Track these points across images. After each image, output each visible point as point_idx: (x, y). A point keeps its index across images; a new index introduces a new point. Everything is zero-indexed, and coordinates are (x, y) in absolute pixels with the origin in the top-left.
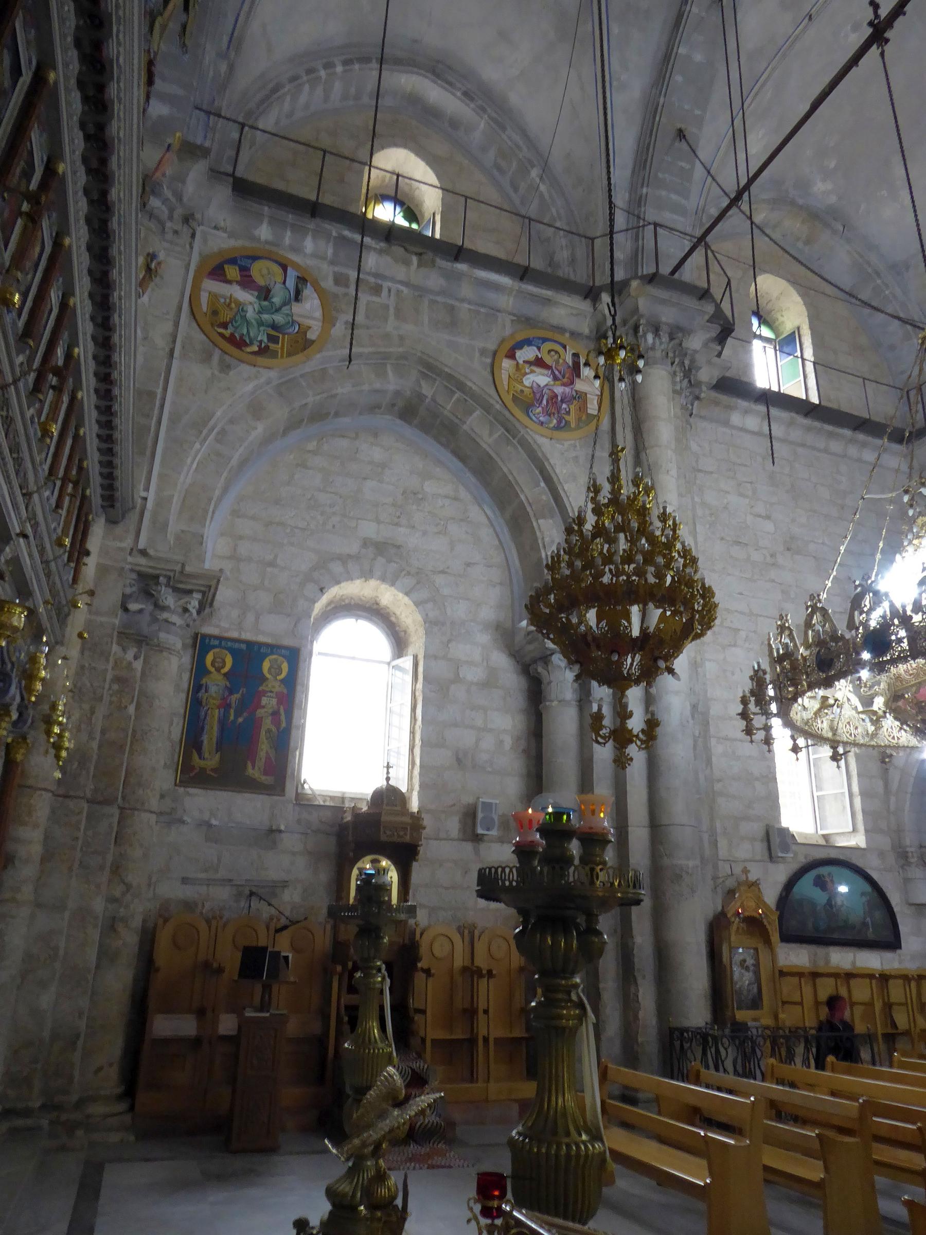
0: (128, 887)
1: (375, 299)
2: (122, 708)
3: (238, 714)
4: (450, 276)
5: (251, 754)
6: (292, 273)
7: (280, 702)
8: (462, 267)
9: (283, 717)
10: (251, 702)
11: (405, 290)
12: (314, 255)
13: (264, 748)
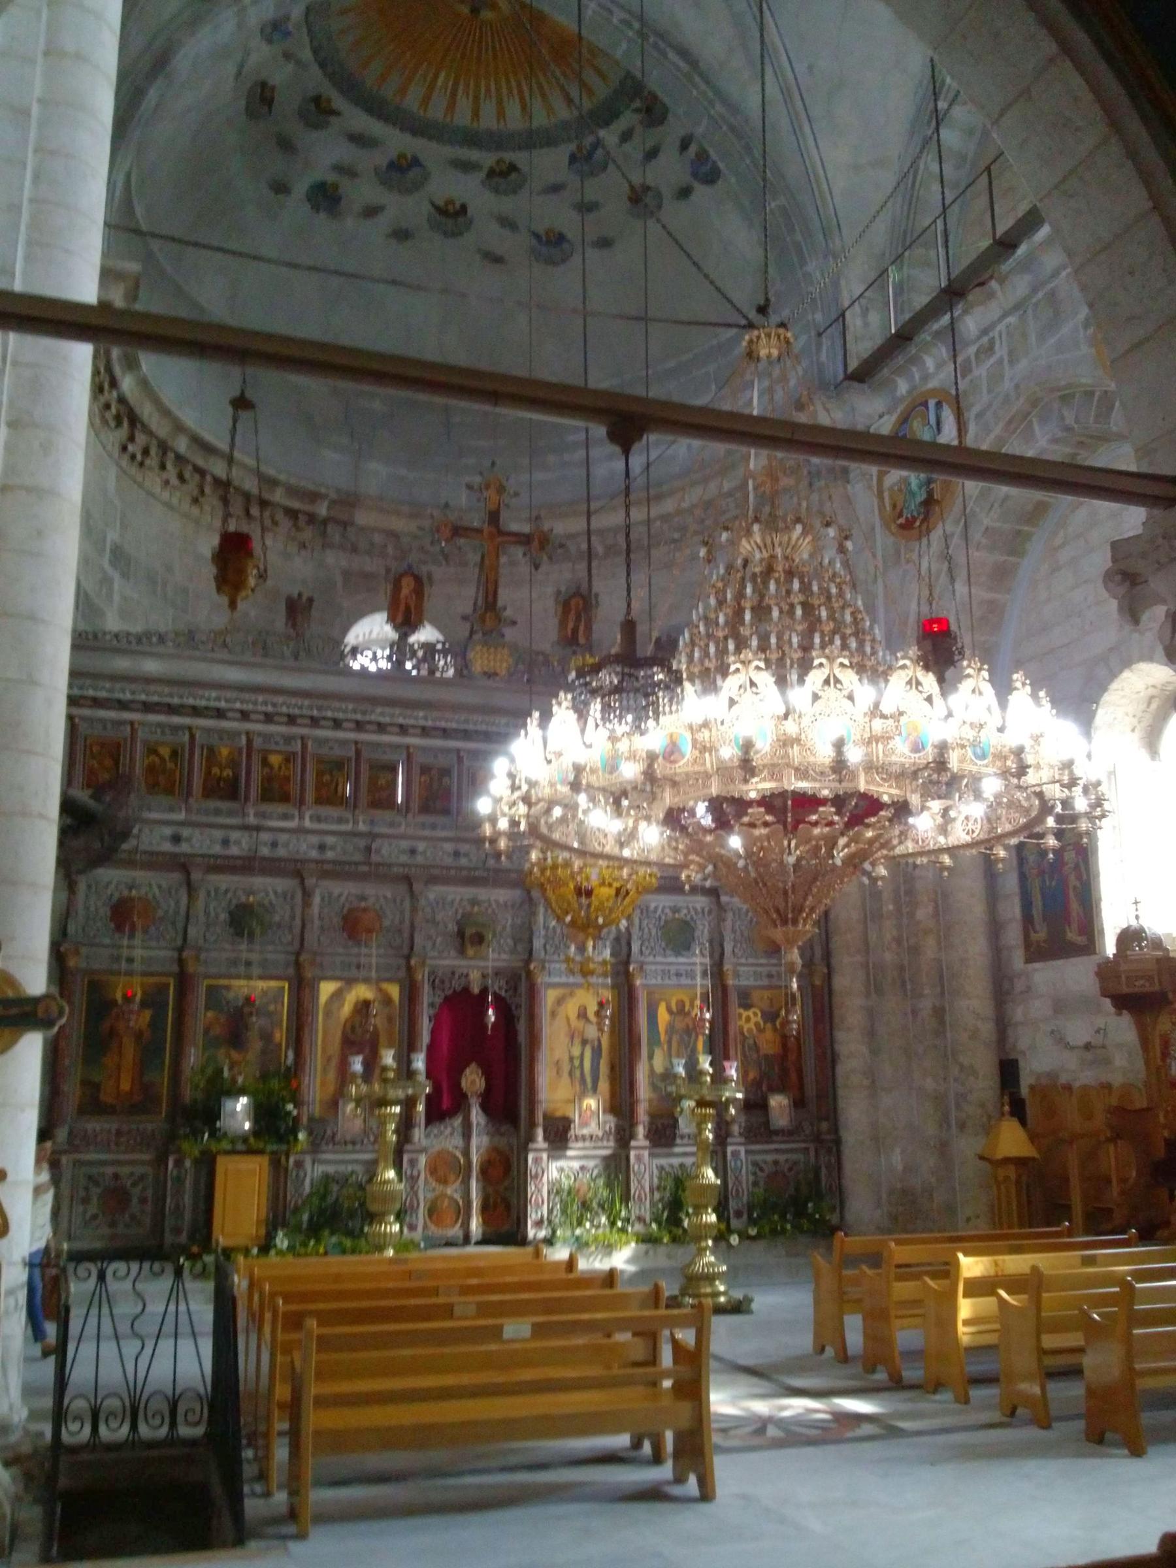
0: (962, 1066)
1: (992, 360)
2: (912, 915)
4: (1027, 265)
6: (932, 403)
8: (1022, 250)
11: (1011, 319)
12: (939, 366)
13: (1075, 906)
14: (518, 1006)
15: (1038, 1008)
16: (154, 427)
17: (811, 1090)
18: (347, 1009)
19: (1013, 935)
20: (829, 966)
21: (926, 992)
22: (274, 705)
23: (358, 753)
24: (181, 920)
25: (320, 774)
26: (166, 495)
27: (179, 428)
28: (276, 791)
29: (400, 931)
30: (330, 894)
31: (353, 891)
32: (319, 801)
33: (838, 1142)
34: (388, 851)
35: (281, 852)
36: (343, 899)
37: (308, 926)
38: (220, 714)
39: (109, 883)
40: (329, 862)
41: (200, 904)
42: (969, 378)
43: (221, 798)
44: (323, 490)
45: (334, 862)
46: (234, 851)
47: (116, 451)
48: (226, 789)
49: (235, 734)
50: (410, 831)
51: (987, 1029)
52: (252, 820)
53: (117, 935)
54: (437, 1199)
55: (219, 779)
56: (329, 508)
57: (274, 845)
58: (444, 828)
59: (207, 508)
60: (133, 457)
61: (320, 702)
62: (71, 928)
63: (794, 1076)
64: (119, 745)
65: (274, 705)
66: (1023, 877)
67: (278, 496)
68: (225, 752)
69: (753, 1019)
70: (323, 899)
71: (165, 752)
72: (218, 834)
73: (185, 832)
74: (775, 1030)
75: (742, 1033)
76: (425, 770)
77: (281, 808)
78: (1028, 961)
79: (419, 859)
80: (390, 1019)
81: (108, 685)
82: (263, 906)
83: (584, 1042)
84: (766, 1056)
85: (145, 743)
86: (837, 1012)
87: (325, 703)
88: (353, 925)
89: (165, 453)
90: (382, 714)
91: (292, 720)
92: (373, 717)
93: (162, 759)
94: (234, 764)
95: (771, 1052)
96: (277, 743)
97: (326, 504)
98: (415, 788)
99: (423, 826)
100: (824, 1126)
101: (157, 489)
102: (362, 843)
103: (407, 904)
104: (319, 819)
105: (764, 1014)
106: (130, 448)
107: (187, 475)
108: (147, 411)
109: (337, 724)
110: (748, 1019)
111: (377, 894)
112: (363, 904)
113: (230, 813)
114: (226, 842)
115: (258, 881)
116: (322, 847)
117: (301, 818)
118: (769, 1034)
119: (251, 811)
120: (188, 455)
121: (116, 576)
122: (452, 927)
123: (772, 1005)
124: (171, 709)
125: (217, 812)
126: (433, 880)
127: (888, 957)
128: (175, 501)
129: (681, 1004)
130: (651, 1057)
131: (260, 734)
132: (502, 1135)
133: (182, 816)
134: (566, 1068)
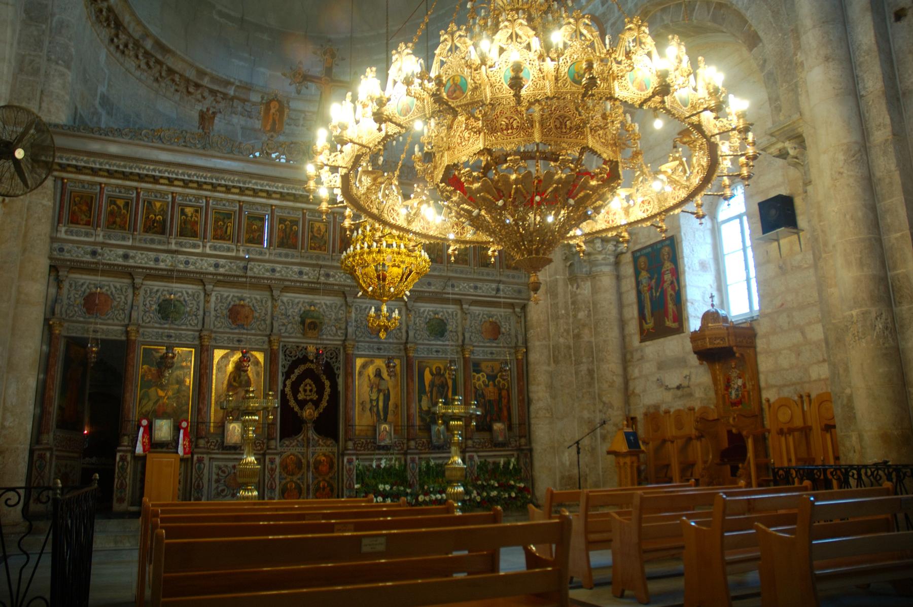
0: (604, 403)
3: (656, 291)
5: (666, 314)
7: (673, 275)
9: (676, 284)
10: (660, 282)
13: (671, 306)
14: (338, 368)
15: (649, 367)
16: (131, 30)
17: (515, 420)
18: (230, 367)
19: (633, 327)
20: (526, 348)
21: (584, 360)
22: (189, 176)
23: (241, 208)
24: (127, 307)
25: (216, 221)
26: (138, 73)
27: (147, 35)
28: (188, 230)
29: (264, 320)
30: (222, 296)
31: (236, 294)
32: (215, 238)
33: (531, 450)
34: (257, 270)
35: (191, 268)
36: (229, 299)
37: (207, 314)
38: (155, 180)
39: (83, 284)
40: (220, 275)
41: (140, 299)
42: (605, 6)
43: (156, 233)
44: (232, 80)
45: (224, 275)
46: (162, 265)
47: (107, 41)
48: (158, 227)
49: (163, 194)
50: (272, 258)
51: (619, 381)
52: (173, 247)
53: (87, 316)
54: (287, 483)
55: (154, 221)
56: (235, 91)
57: (187, 263)
58: (293, 257)
59: (163, 85)
60: (118, 47)
61: (217, 175)
62: (57, 310)
63: (505, 413)
64: (92, 197)
65: (189, 176)
66: (639, 293)
67: (205, 82)
68: (158, 205)
69: (482, 379)
70: (217, 299)
71: (121, 203)
72: (152, 255)
73: (132, 253)
74: (495, 385)
75: (475, 388)
76: (282, 220)
77: (192, 241)
78: (642, 341)
79: (277, 275)
80: (258, 374)
81: (85, 158)
82: (179, 301)
83: (379, 391)
84: (489, 401)
85: (109, 197)
86: (531, 375)
87: (222, 175)
88: (236, 314)
89: (138, 49)
90: (256, 184)
91: (200, 186)
92: (250, 186)
93: (119, 207)
94: (163, 212)
95: (492, 398)
96: (190, 201)
97: (233, 88)
98: (275, 231)
99: (280, 255)
100: (523, 441)
101: (133, 70)
102: (242, 264)
103: (269, 303)
104: (215, 248)
106: (115, 40)
107: (152, 64)
108: (126, 19)
109: (228, 189)
110: (479, 379)
111: (251, 296)
112: (242, 302)
113: (160, 243)
114: (157, 260)
115: (176, 286)
116: (217, 266)
117: (204, 246)
118: (491, 388)
119: (173, 241)
120: (152, 52)
121: (104, 113)
122: (298, 318)
123: (493, 371)
124: (125, 176)
125: (152, 241)
126: (286, 289)
127: (562, 340)
128: (143, 77)
129: (438, 369)
130: (420, 401)
131: (180, 194)
132: (328, 446)
133: (130, 243)
134: (368, 406)
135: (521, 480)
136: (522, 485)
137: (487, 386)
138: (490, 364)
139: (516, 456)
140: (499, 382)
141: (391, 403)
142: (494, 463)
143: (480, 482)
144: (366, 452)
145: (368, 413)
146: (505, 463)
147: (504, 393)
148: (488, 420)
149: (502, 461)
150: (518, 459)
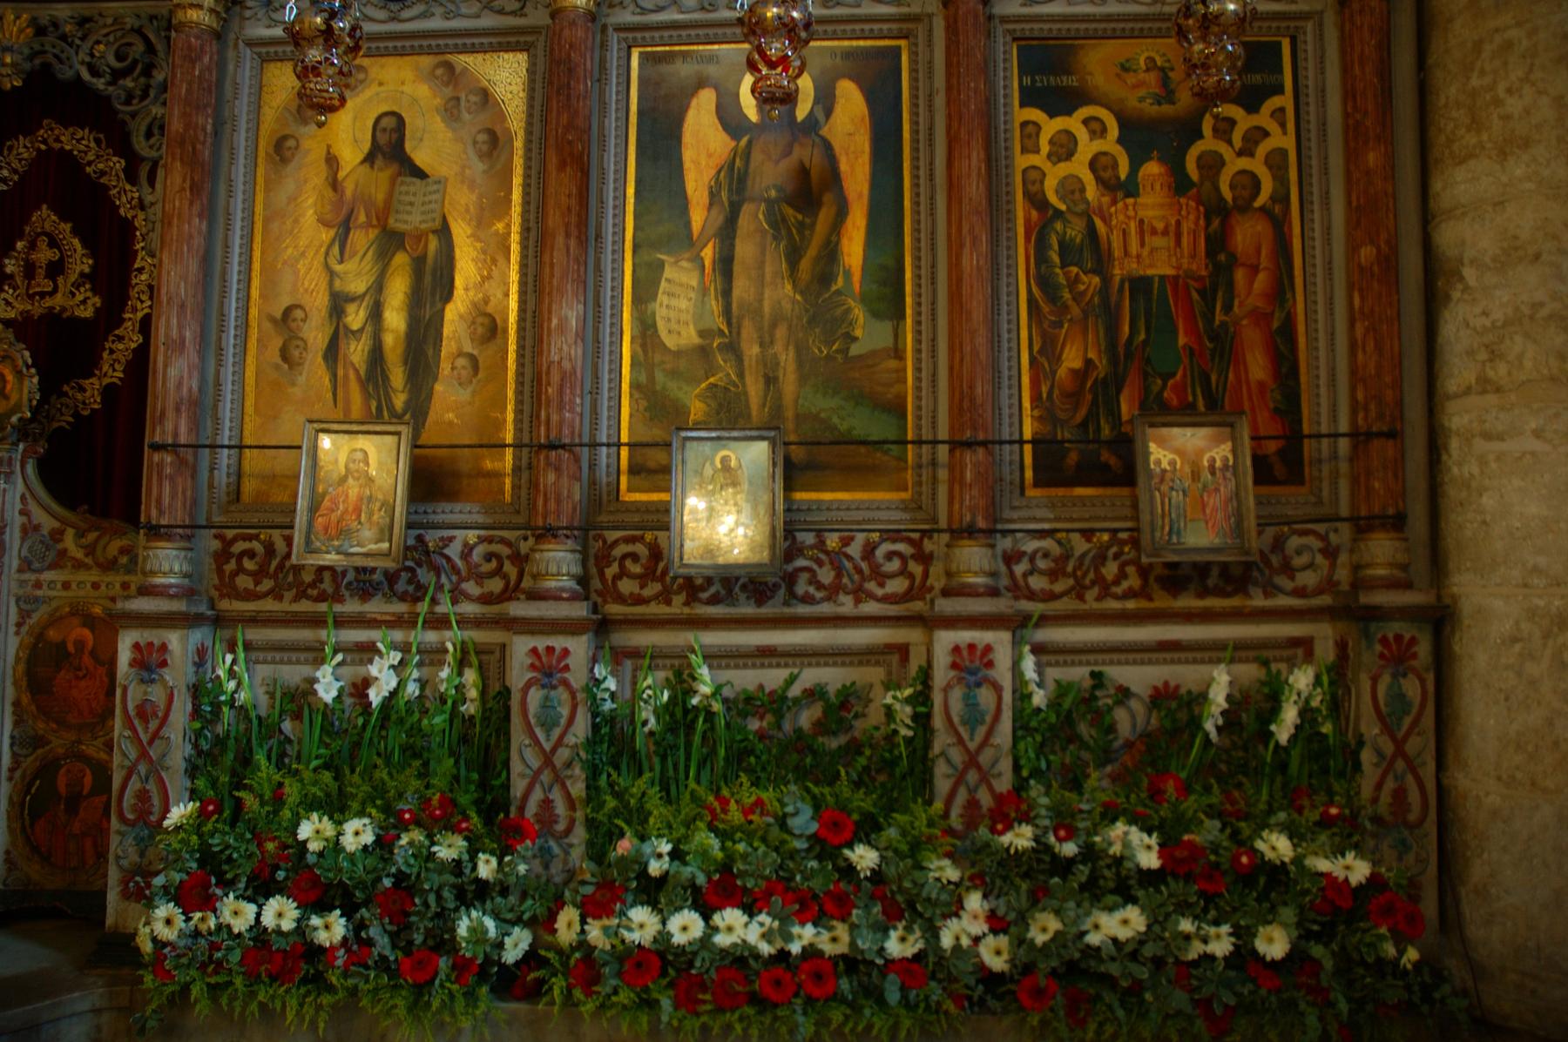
17: (1328, 406)
33: (1441, 620)
63: (1257, 367)
69: (1087, 148)
74: (1179, 184)
75: (1037, 201)
83: (390, 241)
84: (1140, 286)
100: (1382, 550)
105: (1139, 135)
110: (1064, 148)
118: (1153, 203)
123: (1167, 93)
130: (645, 292)
134: (316, 334)
135: (1347, 832)
136: (1358, 870)
137: (1129, 188)
138: (1143, 51)
139: (1326, 651)
140: (1211, 165)
141: (455, 313)
142: (1161, 697)
143: (1020, 838)
144: (286, 606)
145: (315, 371)
146: (1238, 701)
147: (1248, 234)
148: (1126, 408)
149: (1220, 685)
150: (1338, 676)
